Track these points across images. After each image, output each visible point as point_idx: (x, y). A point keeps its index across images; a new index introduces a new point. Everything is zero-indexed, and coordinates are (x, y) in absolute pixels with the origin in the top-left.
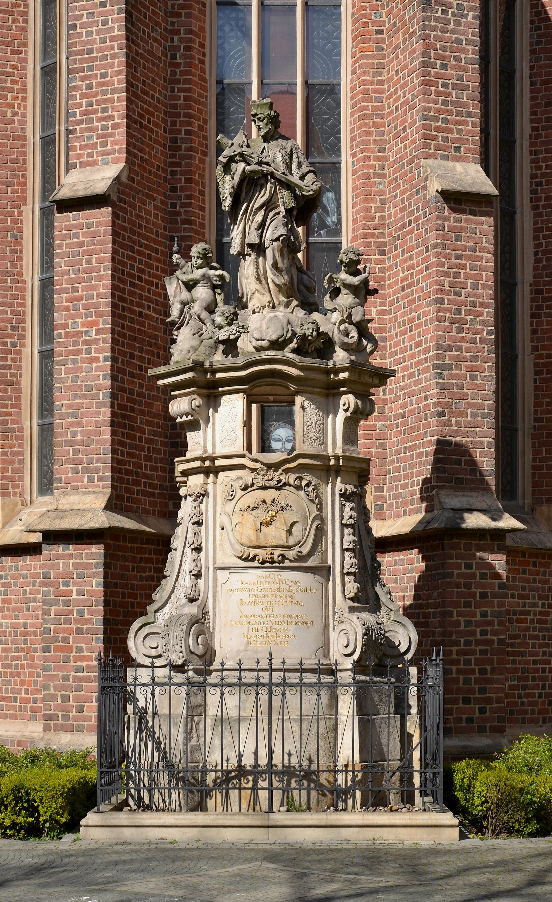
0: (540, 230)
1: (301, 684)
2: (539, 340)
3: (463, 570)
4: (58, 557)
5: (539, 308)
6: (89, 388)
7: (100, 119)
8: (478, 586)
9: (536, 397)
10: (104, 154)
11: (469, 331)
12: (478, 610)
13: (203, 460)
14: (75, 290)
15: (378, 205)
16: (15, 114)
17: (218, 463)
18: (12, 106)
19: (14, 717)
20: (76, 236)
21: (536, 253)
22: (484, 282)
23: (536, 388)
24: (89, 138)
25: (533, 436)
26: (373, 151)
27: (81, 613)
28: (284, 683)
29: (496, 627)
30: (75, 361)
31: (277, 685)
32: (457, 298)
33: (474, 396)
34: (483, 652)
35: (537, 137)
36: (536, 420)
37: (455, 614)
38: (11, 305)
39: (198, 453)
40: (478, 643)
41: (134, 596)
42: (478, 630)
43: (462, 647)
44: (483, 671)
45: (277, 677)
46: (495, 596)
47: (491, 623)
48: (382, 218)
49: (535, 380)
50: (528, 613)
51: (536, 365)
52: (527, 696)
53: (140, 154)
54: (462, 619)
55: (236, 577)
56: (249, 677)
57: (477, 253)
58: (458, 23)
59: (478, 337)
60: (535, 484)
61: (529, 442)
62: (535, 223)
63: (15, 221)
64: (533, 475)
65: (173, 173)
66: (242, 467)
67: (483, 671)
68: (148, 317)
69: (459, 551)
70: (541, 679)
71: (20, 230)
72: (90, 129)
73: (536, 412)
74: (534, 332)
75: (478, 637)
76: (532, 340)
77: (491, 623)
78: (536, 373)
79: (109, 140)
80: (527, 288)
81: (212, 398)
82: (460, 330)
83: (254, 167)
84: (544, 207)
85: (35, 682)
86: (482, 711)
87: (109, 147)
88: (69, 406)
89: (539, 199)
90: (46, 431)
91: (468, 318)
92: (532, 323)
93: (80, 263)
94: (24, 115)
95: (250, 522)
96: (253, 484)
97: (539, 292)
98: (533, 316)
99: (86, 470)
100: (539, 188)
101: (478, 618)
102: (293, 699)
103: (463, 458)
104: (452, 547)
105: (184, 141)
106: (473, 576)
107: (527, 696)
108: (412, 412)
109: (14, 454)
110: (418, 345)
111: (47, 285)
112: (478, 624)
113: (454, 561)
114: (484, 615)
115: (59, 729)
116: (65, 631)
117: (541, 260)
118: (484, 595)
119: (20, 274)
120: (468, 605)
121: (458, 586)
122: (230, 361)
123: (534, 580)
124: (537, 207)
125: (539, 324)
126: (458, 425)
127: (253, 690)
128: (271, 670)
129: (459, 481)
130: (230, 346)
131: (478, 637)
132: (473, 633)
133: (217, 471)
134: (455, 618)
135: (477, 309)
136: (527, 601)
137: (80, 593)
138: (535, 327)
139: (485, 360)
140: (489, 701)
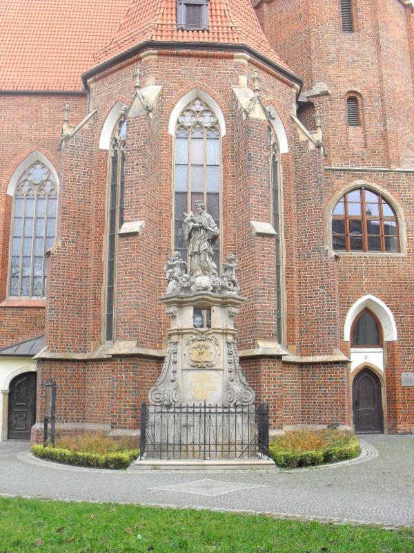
1: (216, 413)
4: (117, 364)
6: (130, 302)
7: (135, 205)
10: (136, 217)
13: (178, 330)
16: (101, 202)
18: (100, 199)
19: (96, 422)
20: (126, 247)
25: (287, 320)
27: (126, 385)
28: (210, 412)
31: (208, 413)
38: (97, 271)
39: (176, 328)
40: (273, 396)
41: (145, 378)
44: (275, 407)
45: (207, 410)
46: (278, 379)
47: (277, 389)
52: (287, 415)
55: (190, 374)
56: (197, 410)
61: (285, 322)
63: (99, 240)
65: (160, 224)
66: (192, 333)
67: (275, 407)
68: (151, 277)
71: (102, 243)
74: (287, 283)
77: (277, 389)
80: (284, 267)
83: (197, 224)
85: (104, 410)
86: (274, 421)
90: (110, 317)
94: (104, 202)
95: (195, 352)
97: (288, 268)
99: (129, 332)
102: (213, 419)
104: (263, 361)
105: (164, 213)
107: (287, 415)
109: (98, 325)
110: (249, 288)
111: (111, 264)
114: (275, 386)
115: (118, 428)
116: (119, 391)
119: (101, 259)
120: (269, 382)
122: (188, 295)
127: (199, 415)
128: (205, 407)
129: (265, 338)
130: (188, 289)
132: (271, 393)
133: (182, 334)
137: (126, 378)
139: (273, 293)
140: (277, 418)
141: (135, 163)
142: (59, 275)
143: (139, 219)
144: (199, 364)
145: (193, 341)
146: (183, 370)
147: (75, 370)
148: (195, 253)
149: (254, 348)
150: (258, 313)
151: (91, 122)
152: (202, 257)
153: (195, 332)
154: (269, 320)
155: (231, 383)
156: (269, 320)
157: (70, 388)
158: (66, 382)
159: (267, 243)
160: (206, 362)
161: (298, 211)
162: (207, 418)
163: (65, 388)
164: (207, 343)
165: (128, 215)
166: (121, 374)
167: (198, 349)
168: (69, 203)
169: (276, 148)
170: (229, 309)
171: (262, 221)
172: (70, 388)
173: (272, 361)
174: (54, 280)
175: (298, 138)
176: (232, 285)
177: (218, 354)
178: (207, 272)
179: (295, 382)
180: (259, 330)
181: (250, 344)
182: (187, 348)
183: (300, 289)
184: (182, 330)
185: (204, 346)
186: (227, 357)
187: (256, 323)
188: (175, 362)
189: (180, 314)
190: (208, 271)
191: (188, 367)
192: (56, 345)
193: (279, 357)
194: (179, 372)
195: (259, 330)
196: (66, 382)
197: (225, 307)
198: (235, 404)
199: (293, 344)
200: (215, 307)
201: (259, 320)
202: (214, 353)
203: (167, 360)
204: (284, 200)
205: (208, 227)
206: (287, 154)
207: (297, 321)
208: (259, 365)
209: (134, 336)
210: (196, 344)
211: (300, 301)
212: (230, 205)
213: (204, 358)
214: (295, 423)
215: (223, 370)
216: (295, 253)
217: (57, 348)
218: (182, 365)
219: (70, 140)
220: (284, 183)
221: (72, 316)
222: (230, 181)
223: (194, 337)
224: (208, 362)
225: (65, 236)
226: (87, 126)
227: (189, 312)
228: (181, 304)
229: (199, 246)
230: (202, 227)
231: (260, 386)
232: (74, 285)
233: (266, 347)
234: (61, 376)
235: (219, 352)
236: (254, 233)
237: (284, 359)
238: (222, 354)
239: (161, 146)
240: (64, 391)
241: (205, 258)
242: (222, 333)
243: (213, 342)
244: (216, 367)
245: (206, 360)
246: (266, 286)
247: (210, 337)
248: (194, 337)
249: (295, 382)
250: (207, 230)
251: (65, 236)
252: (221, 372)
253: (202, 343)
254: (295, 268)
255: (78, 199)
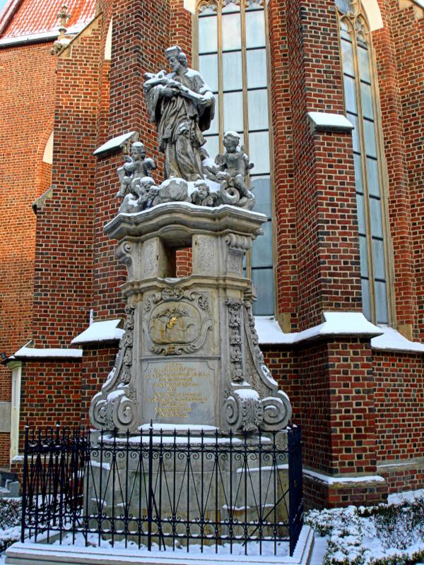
0: (392, 167)
2: (395, 229)
3: (342, 362)
5: (394, 211)
8: (353, 372)
9: (396, 262)
11: (340, 211)
12: (354, 389)
14: (106, 203)
15: (288, 149)
17: (142, 286)
21: (390, 181)
22: (348, 181)
23: (396, 257)
24: (119, 121)
25: (396, 285)
26: (284, 119)
29: (367, 400)
30: (105, 244)
32: (331, 191)
33: (345, 251)
34: (359, 417)
35: (385, 117)
36: (397, 275)
37: (337, 392)
40: (355, 411)
42: (354, 402)
43: (343, 414)
46: (364, 379)
47: (363, 398)
48: (290, 156)
49: (395, 253)
50: (397, 390)
51: (394, 243)
53: (148, 128)
54: (342, 395)
57: (343, 164)
58: (324, 38)
59: (346, 214)
60: (398, 313)
62: (389, 164)
64: (397, 308)
66: (155, 288)
69: (338, 350)
70: (408, 431)
72: (120, 116)
73: (396, 271)
74: (392, 225)
75: (354, 407)
76: (391, 230)
77: (363, 398)
78: (395, 248)
79: (128, 120)
80: (386, 201)
81: (140, 244)
82: (334, 211)
84: (393, 154)
87: (128, 124)
88: (102, 270)
89: (390, 151)
91: (339, 203)
92: (390, 220)
93: (108, 188)
96: (162, 299)
98: (391, 216)
100: (389, 145)
101: (354, 394)
103: (340, 290)
104: (333, 347)
106: (349, 366)
108: (309, 265)
112: (354, 398)
113: (335, 356)
114: (358, 392)
117: (393, 184)
118: (357, 379)
121: (338, 372)
123: (400, 371)
124: (389, 155)
125: (395, 220)
126: (335, 269)
131: (354, 407)
132: (351, 405)
134: (337, 394)
135: (345, 197)
136: (396, 383)
138: (392, 222)
141: (124, 49)
142: (48, 237)
143: (128, 130)
144: (166, 348)
145: (156, 302)
146: (141, 361)
147: (71, 375)
148: (166, 140)
149: (319, 323)
150: (324, 263)
151: (95, 26)
152: (179, 146)
153: (160, 285)
154: (345, 275)
155: (233, 384)
156: (345, 275)
157: (64, 401)
158: (59, 392)
159: (335, 145)
160: (178, 343)
161: (404, 114)
162: (156, 462)
163: (56, 402)
164: (182, 306)
165: (115, 127)
166: (94, 376)
167: (165, 319)
168: (64, 137)
169: (363, 23)
170: (227, 238)
171: (327, 112)
172: (64, 401)
173: (351, 347)
174: (41, 245)
175: (397, 5)
176: (237, 195)
177: (205, 327)
178: (189, 175)
179: (412, 386)
180: (325, 292)
181: (314, 319)
182: (146, 317)
183: (415, 233)
184: (138, 284)
185: (175, 311)
186: (226, 334)
187: (320, 281)
188: (130, 347)
189: (140, 255)
190: (192, 172)
191: (148, 354)
192: (43, 337)
193: (366, 338)
194: (136, 365)
195: (325, 292)
196: (59, 392)
197: (222, 236)
198: (241, 428)
199: (408, 322)
200: (199, 236)
201: (325, 275)
202: (197, 326)
203: (121, 345)
204: (381, 98)
205: (191, 93)
206: (382, 30)
207: (412, 286)
208: (326, 354)
209: (117, 312)
210: (161, 308)
211: (417, 252)
212: (281, 100)
213: (176, 335)
214: (416, 455)
215: (220, 358)
216: (404, 176)
217: (45, 342)
218: (141, 353)
219: (65, 52)
220: (379, 74)
221: (68, 295)
222: (280, 64)
223: (158, 295)
224: (184, 343)
225: (57, 183)
226: (89, 33)
227: (153, 248)
228: (138, 237)
229: (173, 127)
230: (178, 95)
231: (329, 392)
232: (71, 251)
233: (337, 322)
234: (51, 384)
235: (209, 323)
236: (312, 130)
237: (376, 343)
238: (216, 328)
239: (172, 27)
240: (55, 405)
241: (184, 148)
242: (217, 287)
243: (196, 303)
244: (201, 353)
245: (180, 340)
246: (336, 216)
247: (187, 293)
248: (158, 295)
249: (412, 386)
250: (189, 100)
251: (57, 183)
252: (214, 364)
253: (172, 306)
254: (406, 201)
255: (76, 130)
